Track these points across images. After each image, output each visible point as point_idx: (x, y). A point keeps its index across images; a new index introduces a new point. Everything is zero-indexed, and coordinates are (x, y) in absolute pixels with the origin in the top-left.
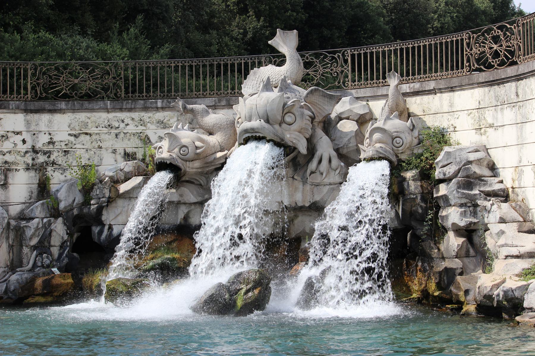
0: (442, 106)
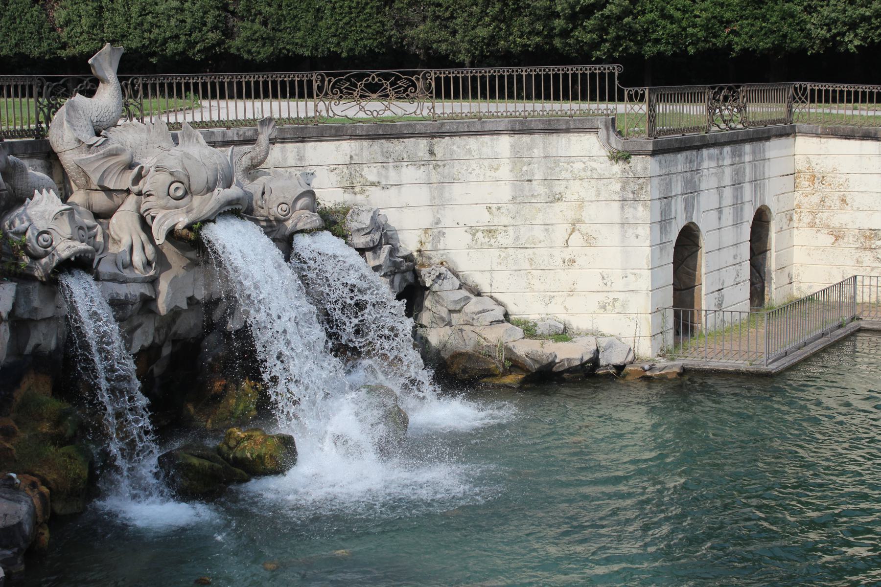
0: (285, 159)
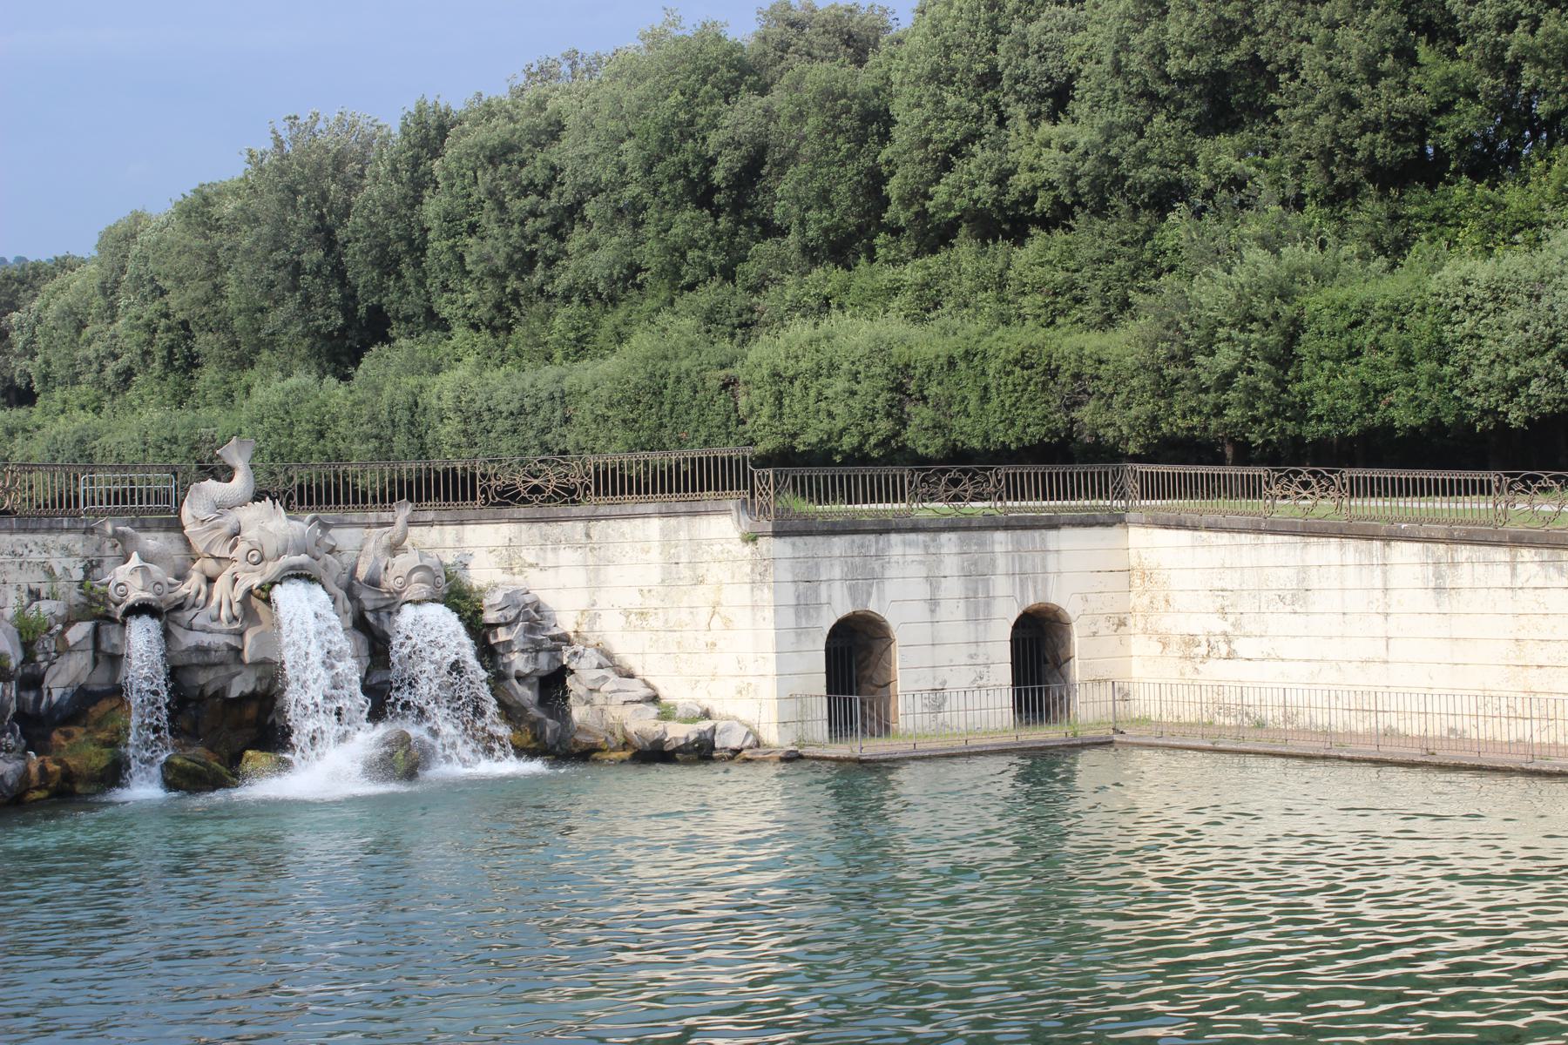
0: (443, 540)
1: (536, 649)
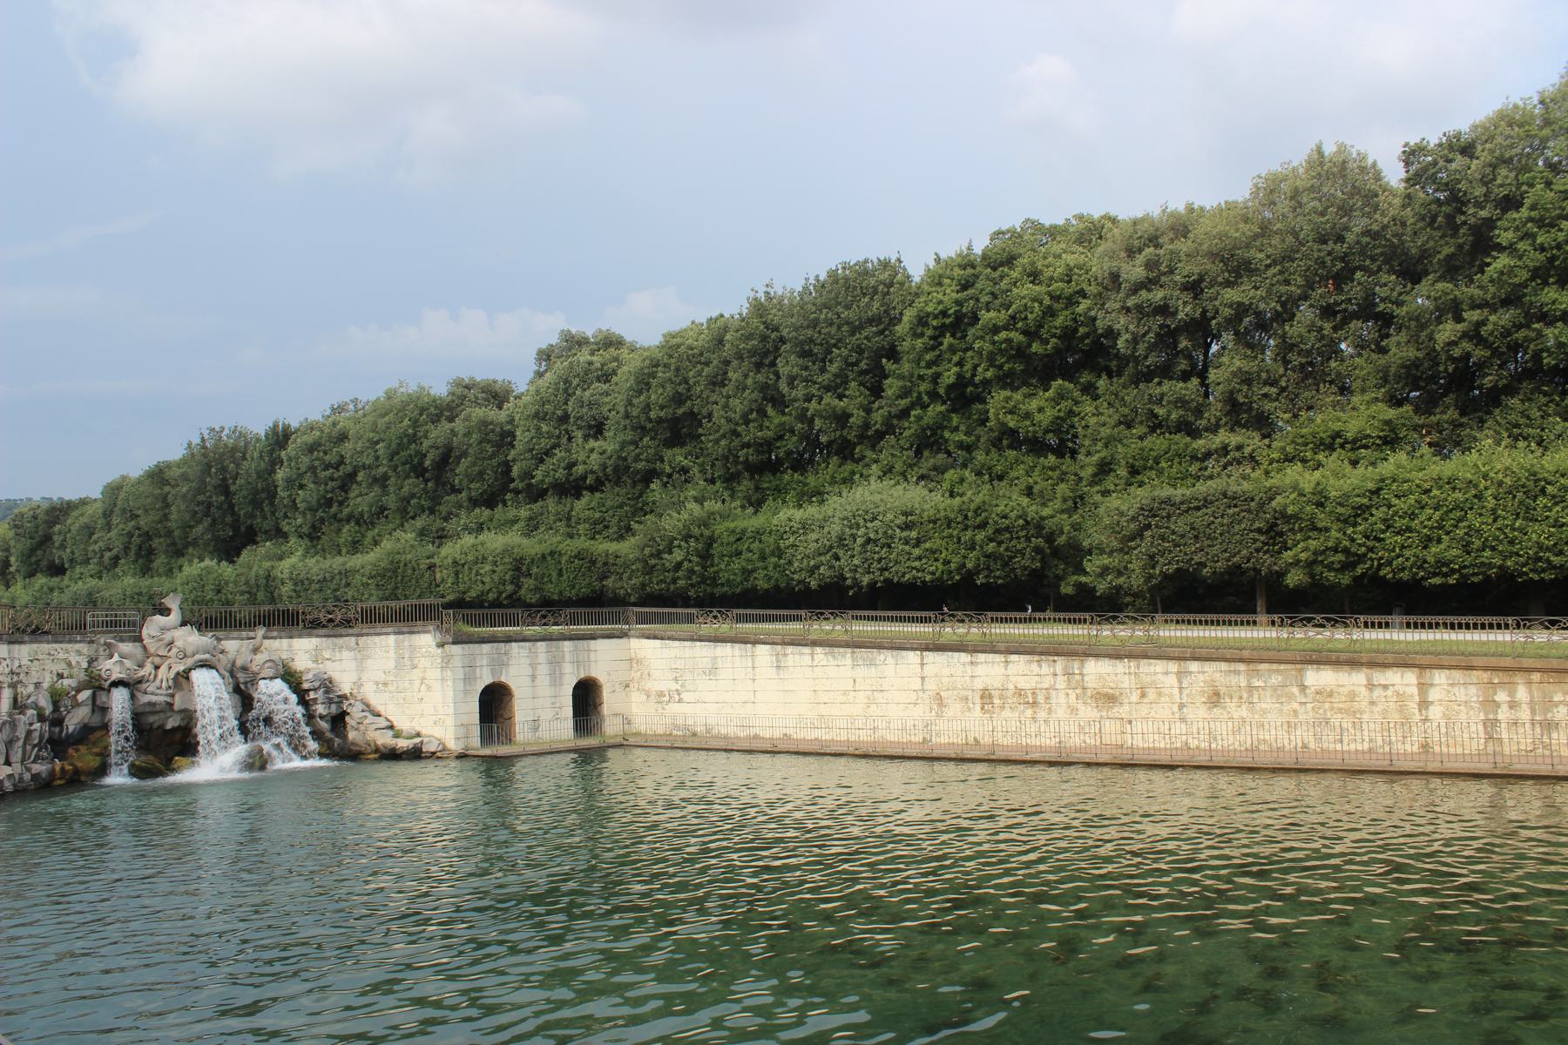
1: (330, 702)
